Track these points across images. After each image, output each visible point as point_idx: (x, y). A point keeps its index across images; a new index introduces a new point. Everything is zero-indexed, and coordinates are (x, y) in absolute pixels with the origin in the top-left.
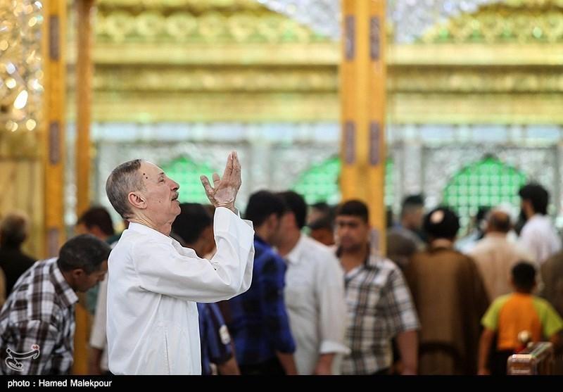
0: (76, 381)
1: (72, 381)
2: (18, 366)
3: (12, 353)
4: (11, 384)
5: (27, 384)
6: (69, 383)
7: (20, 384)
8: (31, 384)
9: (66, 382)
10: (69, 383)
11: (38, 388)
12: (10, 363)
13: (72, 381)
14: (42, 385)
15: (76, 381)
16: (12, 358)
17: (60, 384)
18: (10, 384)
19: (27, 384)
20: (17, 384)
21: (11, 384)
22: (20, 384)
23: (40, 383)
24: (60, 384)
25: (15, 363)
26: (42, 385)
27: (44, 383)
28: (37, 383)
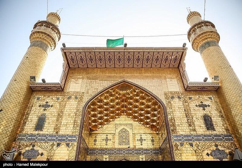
0: (33, 163)
1: (31, 163)
2: (8, 157)
3: (5, 151)
4: (4, 165)
5: (12, 165)
6: (29, 164)
7: (8, 165)
8: (13, 165)
9: (28, 164)
10: (29, 164)
11: (16, 166)
12: (4, 156)
13: (31, 163)
14: (18, 165)
15: (33, 163)
16: (5, 153)
17: (25, 165)
18: (4, 165)
19: (12, 165)
20: (7, 165)
21: (4, 165)
22: (8, 165)
23: (17, 164)
24: (25, 165)
25: (6, 156)
26: (18, 165)
27: (19, 164)
28: (16, 165)
